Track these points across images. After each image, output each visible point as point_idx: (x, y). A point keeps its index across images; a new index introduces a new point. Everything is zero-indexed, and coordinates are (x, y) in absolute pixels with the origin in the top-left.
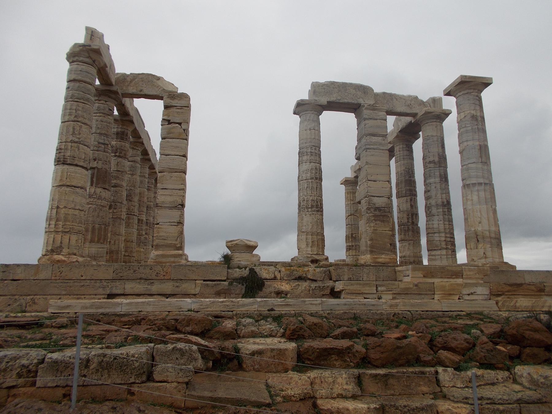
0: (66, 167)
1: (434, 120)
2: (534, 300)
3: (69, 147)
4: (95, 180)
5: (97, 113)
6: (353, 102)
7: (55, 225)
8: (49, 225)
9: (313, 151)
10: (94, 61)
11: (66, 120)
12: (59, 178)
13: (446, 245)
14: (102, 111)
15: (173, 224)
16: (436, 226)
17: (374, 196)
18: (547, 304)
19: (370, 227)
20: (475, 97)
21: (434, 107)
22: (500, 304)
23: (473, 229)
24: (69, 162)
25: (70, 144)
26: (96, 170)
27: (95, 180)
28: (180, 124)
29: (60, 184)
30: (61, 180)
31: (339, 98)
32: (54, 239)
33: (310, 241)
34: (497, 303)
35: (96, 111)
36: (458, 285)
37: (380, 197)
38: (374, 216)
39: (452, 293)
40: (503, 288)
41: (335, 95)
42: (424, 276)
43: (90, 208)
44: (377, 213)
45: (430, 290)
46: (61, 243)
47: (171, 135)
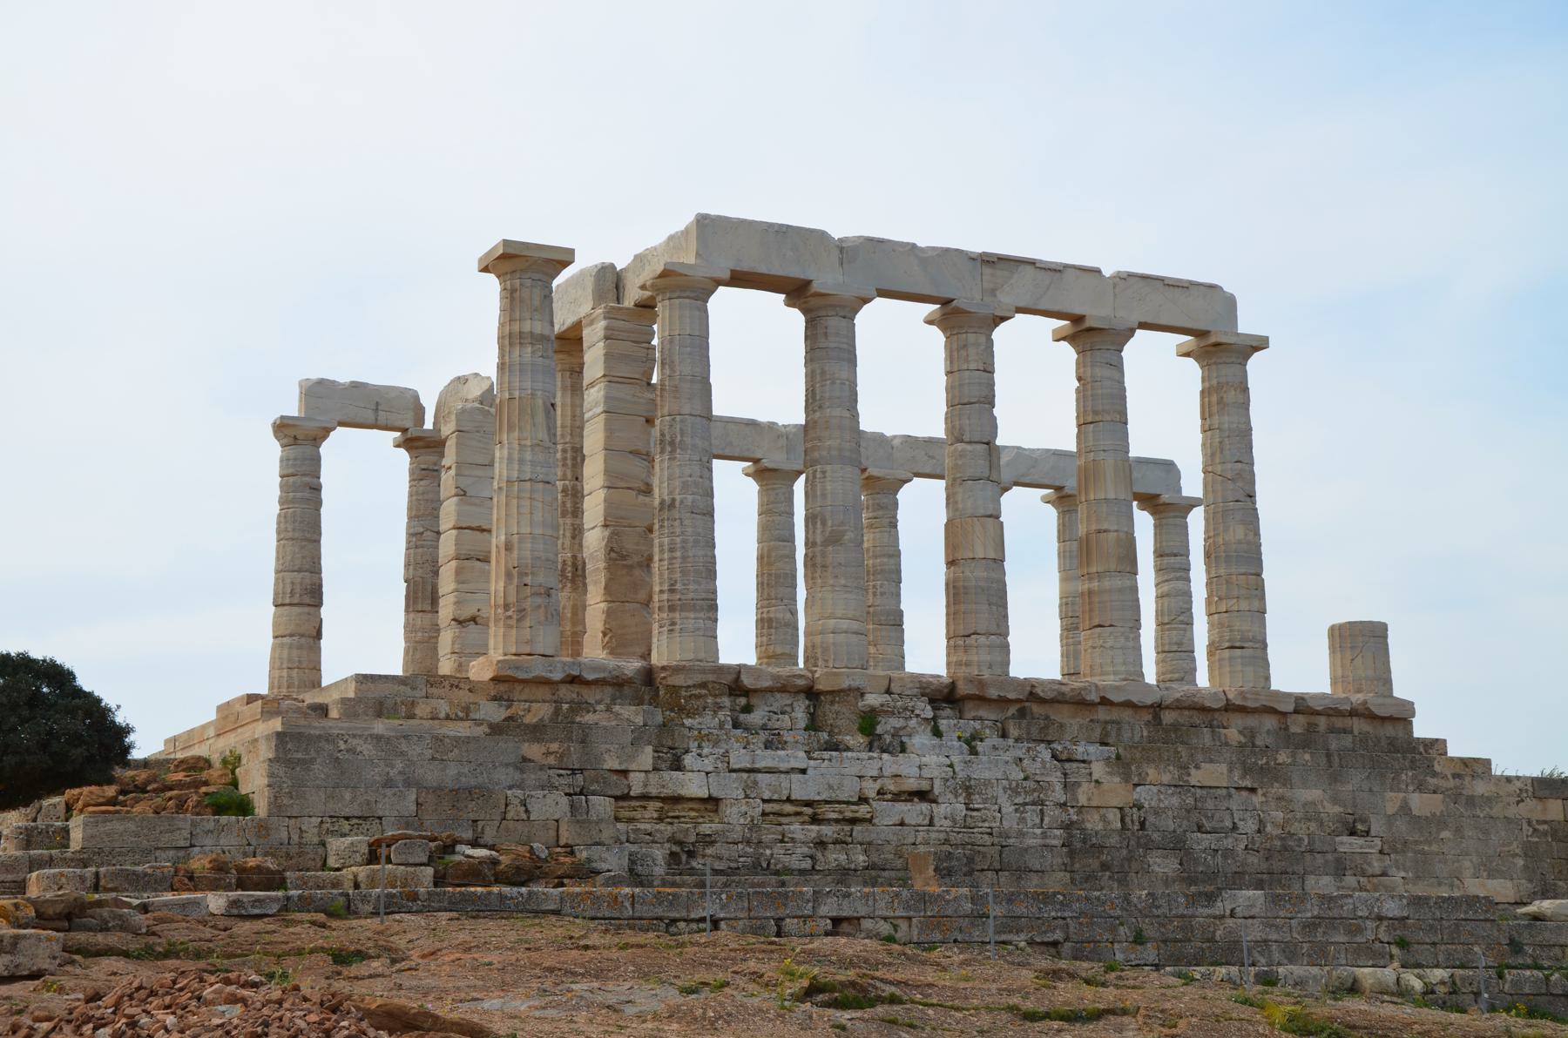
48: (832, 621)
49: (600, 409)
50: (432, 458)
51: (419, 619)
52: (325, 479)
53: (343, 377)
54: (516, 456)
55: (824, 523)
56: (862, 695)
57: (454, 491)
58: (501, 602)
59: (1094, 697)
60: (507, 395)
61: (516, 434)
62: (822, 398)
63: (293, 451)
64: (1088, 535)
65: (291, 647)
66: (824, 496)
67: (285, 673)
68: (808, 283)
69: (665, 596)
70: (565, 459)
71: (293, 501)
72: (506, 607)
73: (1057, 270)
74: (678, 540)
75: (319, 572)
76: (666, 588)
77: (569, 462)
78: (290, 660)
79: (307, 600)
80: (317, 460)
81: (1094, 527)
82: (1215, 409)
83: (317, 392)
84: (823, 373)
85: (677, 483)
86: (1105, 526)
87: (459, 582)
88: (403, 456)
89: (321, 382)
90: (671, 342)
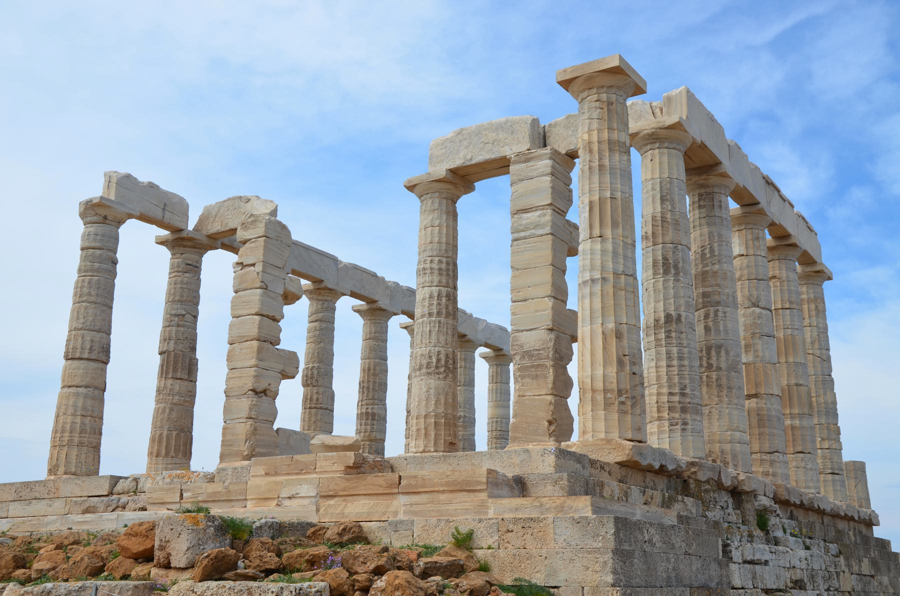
1: (649, 147)
2: (372, 502)
6: (493, 156)
9: (428, 266)
10: (105, 218)
13: (659, 411)
15: (241, 421)
17: (523, 331)
18: (392, 509)
20: (594, 104)
21: (669, 114)
22: (322, 511)
28: (253, 265)
31: (469, 157)
34: (318, 510)
36: (276, 483)
37: (531, 330)
39: (267, 496)
40: (337, 484)
41: (461, 155)
42: (267, 474)
44: (527, 362)
45: (241, 494)
47: (243, 286)
48: (738, 434)
49: (548, 230)
50: (196, 257)
51: (177, 386)
52: (119, 255)
53: (143, 176)
54: (621, 251)
55: (727, 353)
56: (755, 496)
57: (259, 284)
58: (614, 386)
59: (816, 506)
60: (608, 194)
61: (620, 231)
62: (720, 255)
63: (92, 229)
64: (788, 385)
65: (86, 396)
66: (726, 331)
67: (78, 420)
68: (718, 163)
69: (676, 398)
70: (448, 270)
71: (98, 270)
72: (620, 392)
73: (783, 199)
74: (686, 350)
75: (108, 333)
76: (677, 390)
77: (451, 273)
78: (84, 408)
79: (104, 358)
80: (115, 239)
81: (793, 381)
82: (814, 313)
83: (125, 183)
84: (720, 235)
85: (682, 301)
86: (801, 382)
87: (260, 359)
88: (165, 253)
89: (128, 177)
90: (671, 183)
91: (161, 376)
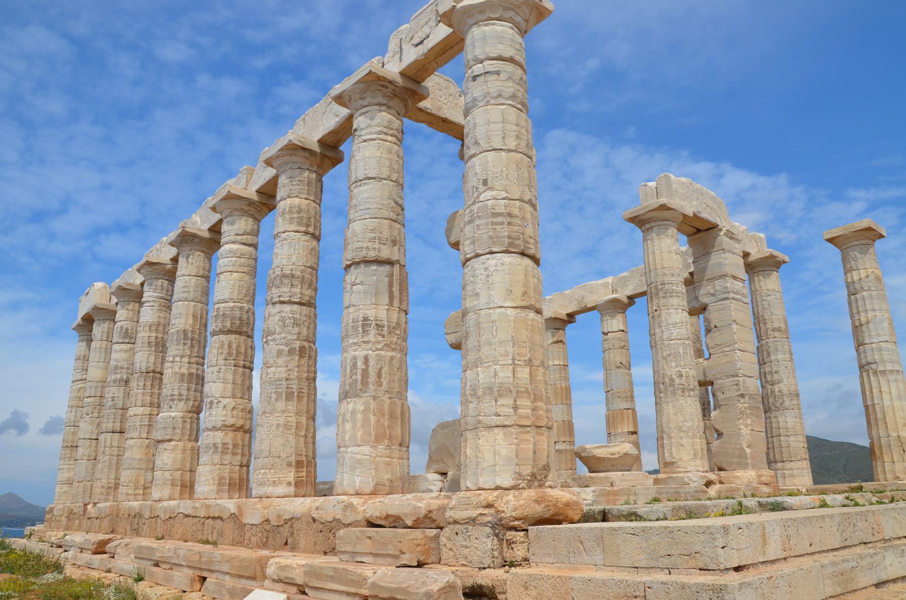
0: (527, 261)
3: (528, 216)
4: (396, 289)
5: (386, 134)
7: (534, 410)
8: (516, 408)
11: (513, 148)
12: (518, 291)
14: (396, 133)
16: (790, 425)
19: (747, 425)
23: (894, 434)
24: (531, 252)
25: (529, 208)
26: (396, 268)
27: (396, 289)
29: (524, 303)
30: (525, 293)
32: (535, 445)
33: (698, 448)
35: (385, 130)
38: (750, 408)
41: (695, 203)
43: (392, 358)
46: (548, 457)
91: (391, 303)
